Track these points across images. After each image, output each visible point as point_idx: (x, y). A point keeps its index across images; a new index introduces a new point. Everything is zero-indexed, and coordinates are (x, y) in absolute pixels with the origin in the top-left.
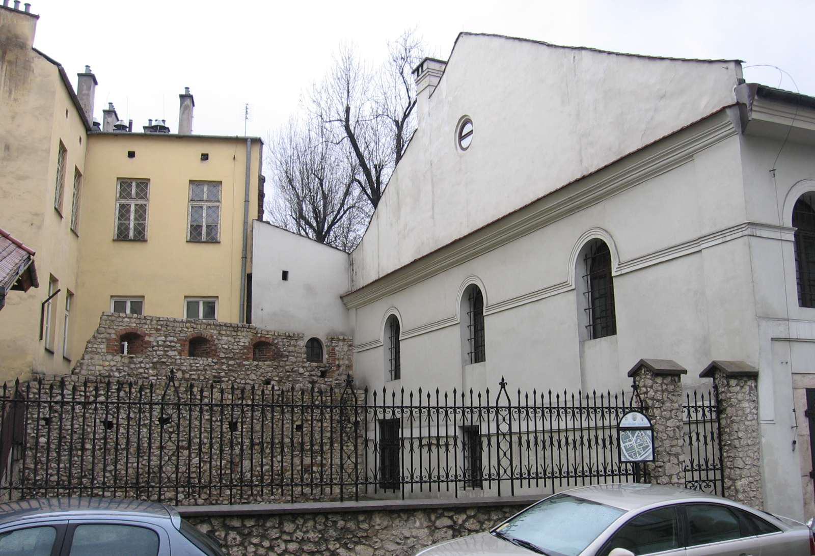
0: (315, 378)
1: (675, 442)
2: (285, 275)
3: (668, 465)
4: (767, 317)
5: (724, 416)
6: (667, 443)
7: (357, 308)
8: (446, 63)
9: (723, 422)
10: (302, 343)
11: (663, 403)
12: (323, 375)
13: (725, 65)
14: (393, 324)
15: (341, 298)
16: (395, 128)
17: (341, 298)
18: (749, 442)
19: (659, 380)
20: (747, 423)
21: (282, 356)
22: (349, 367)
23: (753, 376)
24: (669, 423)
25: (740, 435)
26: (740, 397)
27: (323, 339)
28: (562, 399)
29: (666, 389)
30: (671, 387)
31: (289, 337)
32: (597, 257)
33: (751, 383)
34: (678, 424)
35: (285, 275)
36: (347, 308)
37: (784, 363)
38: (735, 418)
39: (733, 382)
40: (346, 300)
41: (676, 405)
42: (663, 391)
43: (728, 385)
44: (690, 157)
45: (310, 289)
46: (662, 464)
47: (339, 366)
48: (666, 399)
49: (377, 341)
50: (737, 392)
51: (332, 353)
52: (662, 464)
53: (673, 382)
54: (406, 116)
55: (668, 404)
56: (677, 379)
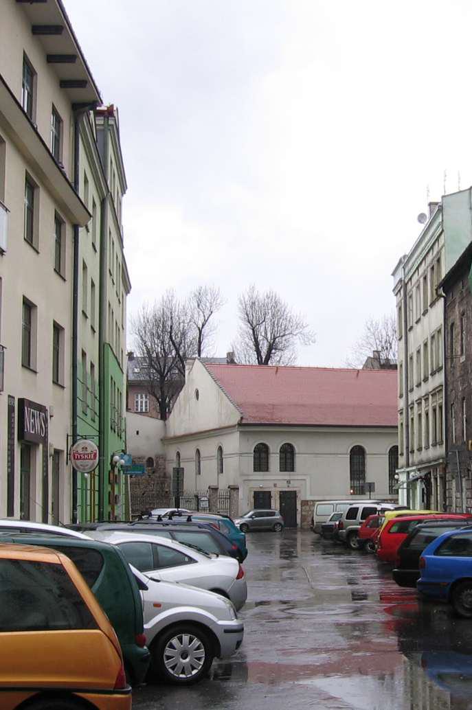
2: (138, 433)
4: (242, 475)
10: (145, 460)
12: (154, 472)
14: (178, 454)
15: (162, 440)
16: (198, 331)
17: (162, 440)
22: (165, 469)
23: (238, 489)
27: (154, 458)
31: (139, 458)
35: (138, 433)
36: (164, 444)
45: (148, 438)
49: (173, 460)
50: (234, 493)
51: (157, 463)
54: (203, 326)
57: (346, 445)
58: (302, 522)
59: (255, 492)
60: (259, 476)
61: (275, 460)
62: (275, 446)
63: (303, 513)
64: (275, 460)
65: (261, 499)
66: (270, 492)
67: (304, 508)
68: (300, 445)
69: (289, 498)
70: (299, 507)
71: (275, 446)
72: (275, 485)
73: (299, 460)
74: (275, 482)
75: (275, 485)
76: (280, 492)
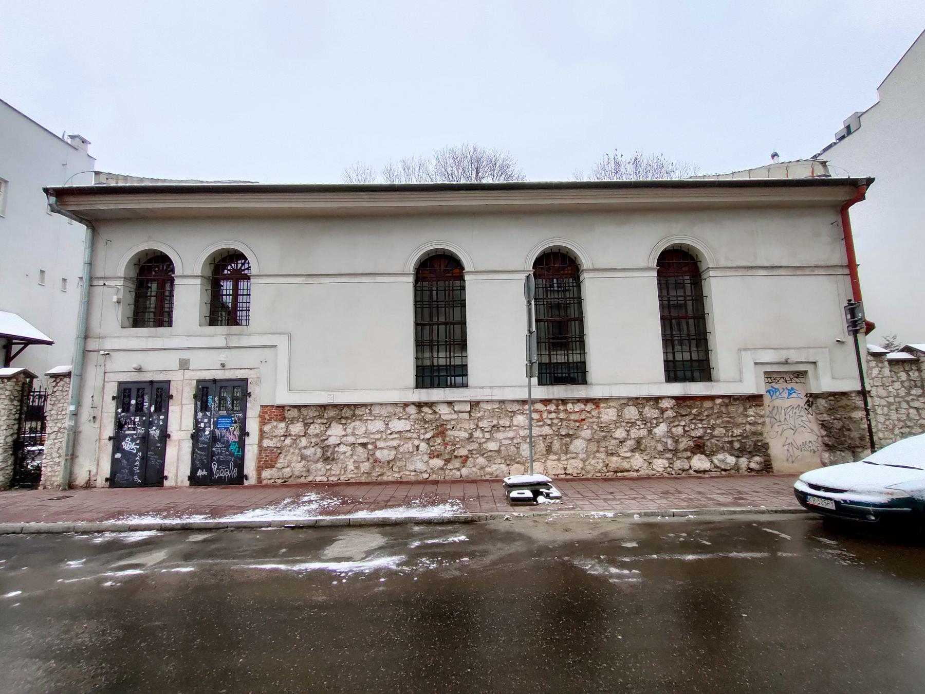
57: (404, 250)
60: (146, 337)
62: (190, 256)
63: (266, 443)
64: (188, 297)
65: (142, 400)
67: (267, 428)
68: (262, 251)
69: (222, 396)
70: (252, 426)
71: (190, 256)
72: (184, 365)
73: (260, 296)
74: (185, 355)
75: (184, 365)
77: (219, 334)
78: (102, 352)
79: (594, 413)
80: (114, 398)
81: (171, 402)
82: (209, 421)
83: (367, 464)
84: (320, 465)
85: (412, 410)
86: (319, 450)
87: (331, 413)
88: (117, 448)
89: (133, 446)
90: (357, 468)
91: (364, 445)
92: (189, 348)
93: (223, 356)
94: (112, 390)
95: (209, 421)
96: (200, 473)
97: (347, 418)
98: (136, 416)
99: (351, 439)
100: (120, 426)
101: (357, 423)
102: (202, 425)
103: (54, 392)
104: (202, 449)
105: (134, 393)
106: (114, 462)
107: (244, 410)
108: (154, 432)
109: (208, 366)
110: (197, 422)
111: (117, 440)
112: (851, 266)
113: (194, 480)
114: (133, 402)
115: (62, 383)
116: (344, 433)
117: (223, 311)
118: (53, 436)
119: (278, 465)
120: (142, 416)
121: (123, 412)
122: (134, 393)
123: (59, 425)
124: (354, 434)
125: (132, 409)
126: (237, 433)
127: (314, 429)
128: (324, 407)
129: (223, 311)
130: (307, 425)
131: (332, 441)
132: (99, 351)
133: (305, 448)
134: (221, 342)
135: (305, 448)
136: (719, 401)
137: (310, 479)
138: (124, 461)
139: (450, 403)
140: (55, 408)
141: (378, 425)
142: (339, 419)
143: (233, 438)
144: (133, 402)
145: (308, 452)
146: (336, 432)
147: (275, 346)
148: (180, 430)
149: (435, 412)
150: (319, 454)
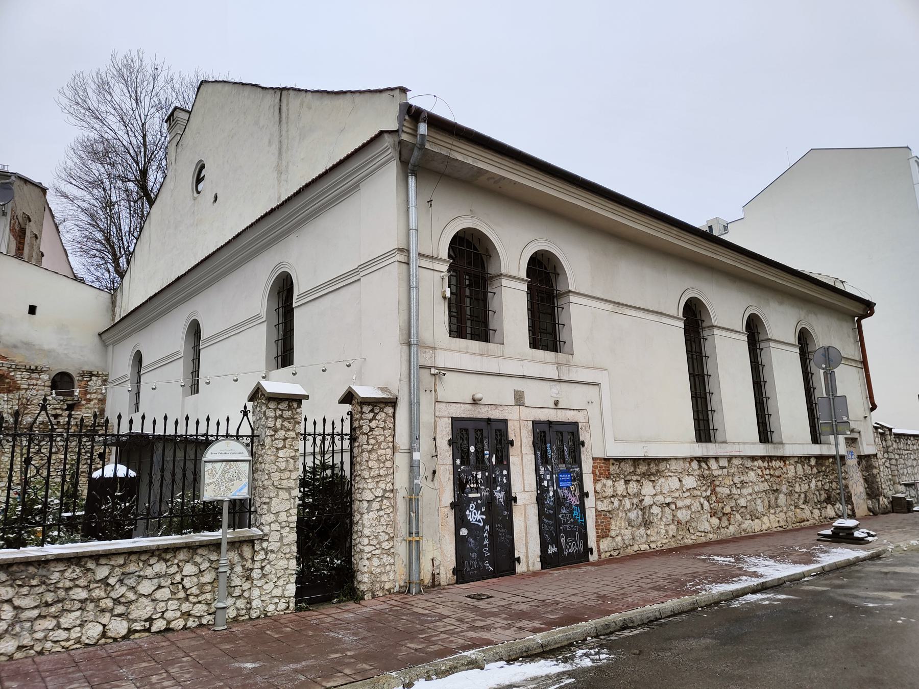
0: (59, 412)
1: (286, 475)
3: (274, 502)
5: (356, 444)
6: (276, 476)
7: (115, 343)
8: (190, 113)
9: (356, 451)
10: (45, 377)
11: (276, 431)
13: (392, 93)
15: (100, 335)
18: (382, 472)
19: (272, 405)
20: (380, 452)
21: (19, 389)
22: (103, 401)
24: (281, 453)
25: (371, 464)
26: (373, 424)
27: (74, 374)
28: (203, 424)
29: (281, 416)
30: (287, 414)
32: (284, 290)
33: (390, 410)
34: (293, 454)
37: (428, 392)
38: (365, 446)
39: (366, 409)
40: (104, 337)
41: (293, 434)
42: (276, 418)
43: (362, 413)
44: (356, 187)
46: (268, 500)
47: (90, 400)
48: (278, 426)
52: (268, 500)
53: (290, 408)
55: (281, 433)
56: (295, 405)
58: (599, 538)
59: (454, 420)
60: (464, 354)
61: (512, 304)
64: (512, 304)
66: (505, 422)
67: (599, 486)
69: (558, 442)
70: (588, 485)
72: (519, 399)
73: (579, 318)
75: (519, 399)
76: (535, 423)
77: (542, 362)
78: (433, 371)
79: (785, 470)
80: (512, 443)
81: (512, 451)
82: (552, 478)
83: (673, 526)
84: (642, 530)
85: (695, 465)
86: (640, 513)
87: (643, 468)
88: (461, 521)
89: (479, 517)
90: (667, 532)
91: (668, 504)
92: (524, 377)
93: (554, 391)
94: (445, 433)
95: (552, 478)
96: (552, 550)
97: (652, 474)
98: (477, 470)
99: (660, 499)
100: (460, 485)
101: (662, 480)
102: (545, 483)
103: (372, 429)
104: (549, 517)
105: (472, 435)
106: (460, 541)
107: (577, 461)
108: (499, 495)
109: (541, 403)
110: (539, 480)
111: (459, 507)
112: (865, 362)
113: (548, 561)
114: (472, 449)
115: (381, 416)
116: (654, 492)
117: (546, 332)
118: (376, 505)
119: (613, 533)
120: (483, 470)
121: (462, 463)
122: (472, 435)
123: (382, 485)
124: (662, 493)
125: (472, 459)
126: (577, 493)
127: (633, 487)
128: (636, 461)
129: (546, 332)
130: (627, 482)
131: (648, 501)
132: (430, 368)
133: (629, 510)
134: (552, 373)
135: (629, 510)
136: (831, 460)
137: (636, 548)
138: (471, 540)
139: (716, 458)
140: (374, 456)
141: (674, 483)
142: (647, 475)
143: (575, 501)
144: (472, 449)
145: (632, 515)
146: (648, 489)
147: (597, 384)
148: (524, 491)
149: (709, 468)
150: (640, 519)
